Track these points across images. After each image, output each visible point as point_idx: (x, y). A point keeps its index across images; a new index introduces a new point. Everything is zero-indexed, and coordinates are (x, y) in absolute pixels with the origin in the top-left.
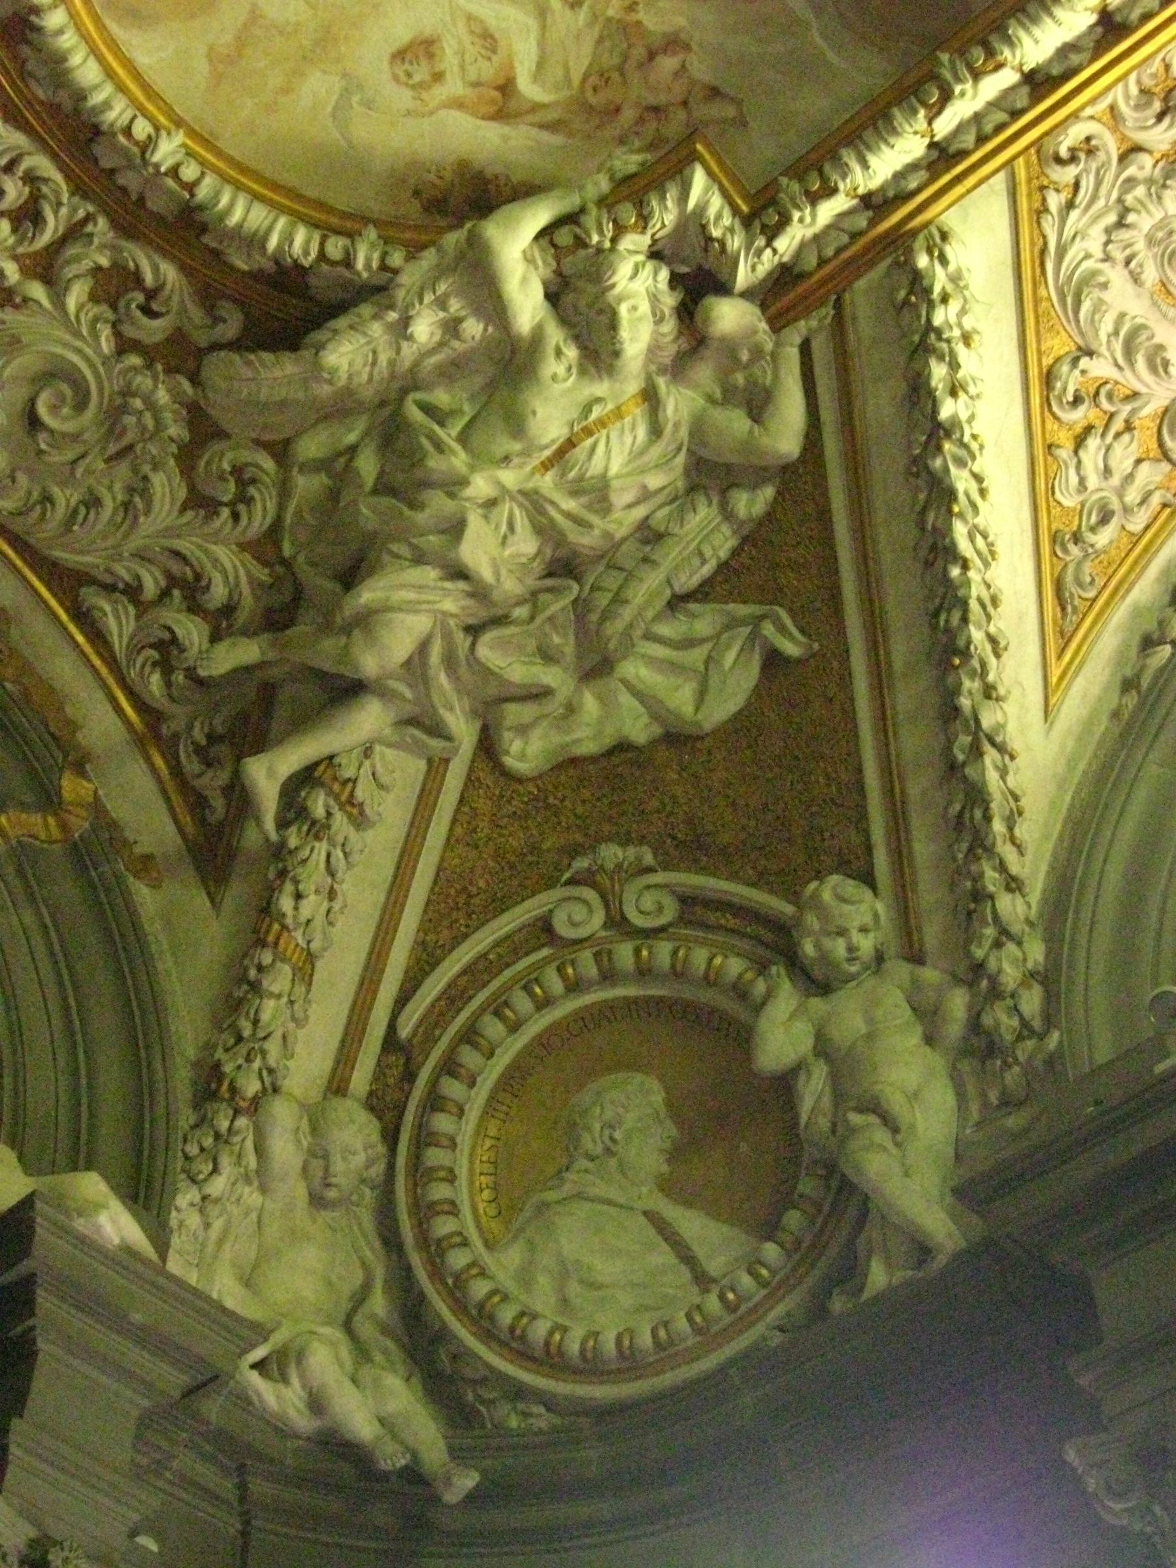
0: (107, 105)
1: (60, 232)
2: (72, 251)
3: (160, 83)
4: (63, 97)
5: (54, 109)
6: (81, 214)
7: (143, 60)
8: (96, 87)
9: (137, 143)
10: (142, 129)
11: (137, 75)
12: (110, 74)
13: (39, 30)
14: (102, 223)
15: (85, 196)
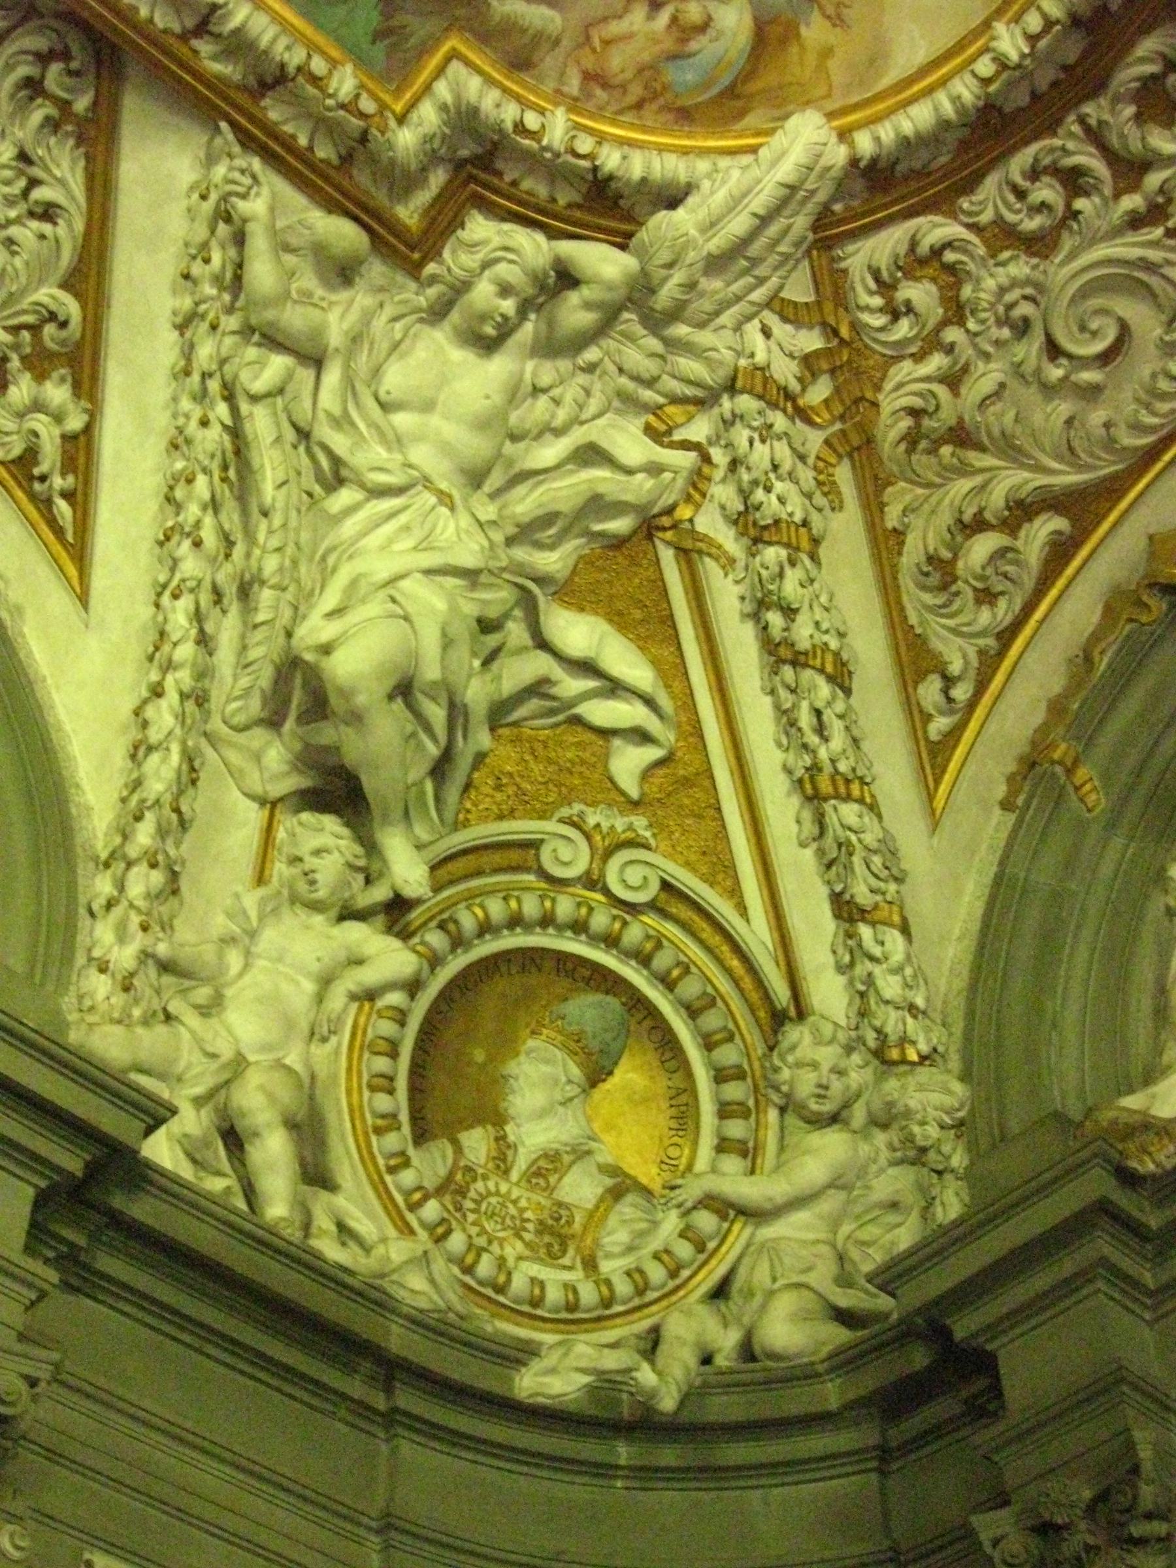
0: (956, 99)
1: (1093, 150)
2: (1114, 141)
3: (946, 42)
4: (951, 138)
5: (964, 145)
6: (1076, 128)
7: (921, 55)
8: (936, 109)
9: (998, 74)
10: (985, 67)
11: (936, 63)
12: (929, 91)
13: (874, 161)
14: (1088, 109)
15: (1059, 122)
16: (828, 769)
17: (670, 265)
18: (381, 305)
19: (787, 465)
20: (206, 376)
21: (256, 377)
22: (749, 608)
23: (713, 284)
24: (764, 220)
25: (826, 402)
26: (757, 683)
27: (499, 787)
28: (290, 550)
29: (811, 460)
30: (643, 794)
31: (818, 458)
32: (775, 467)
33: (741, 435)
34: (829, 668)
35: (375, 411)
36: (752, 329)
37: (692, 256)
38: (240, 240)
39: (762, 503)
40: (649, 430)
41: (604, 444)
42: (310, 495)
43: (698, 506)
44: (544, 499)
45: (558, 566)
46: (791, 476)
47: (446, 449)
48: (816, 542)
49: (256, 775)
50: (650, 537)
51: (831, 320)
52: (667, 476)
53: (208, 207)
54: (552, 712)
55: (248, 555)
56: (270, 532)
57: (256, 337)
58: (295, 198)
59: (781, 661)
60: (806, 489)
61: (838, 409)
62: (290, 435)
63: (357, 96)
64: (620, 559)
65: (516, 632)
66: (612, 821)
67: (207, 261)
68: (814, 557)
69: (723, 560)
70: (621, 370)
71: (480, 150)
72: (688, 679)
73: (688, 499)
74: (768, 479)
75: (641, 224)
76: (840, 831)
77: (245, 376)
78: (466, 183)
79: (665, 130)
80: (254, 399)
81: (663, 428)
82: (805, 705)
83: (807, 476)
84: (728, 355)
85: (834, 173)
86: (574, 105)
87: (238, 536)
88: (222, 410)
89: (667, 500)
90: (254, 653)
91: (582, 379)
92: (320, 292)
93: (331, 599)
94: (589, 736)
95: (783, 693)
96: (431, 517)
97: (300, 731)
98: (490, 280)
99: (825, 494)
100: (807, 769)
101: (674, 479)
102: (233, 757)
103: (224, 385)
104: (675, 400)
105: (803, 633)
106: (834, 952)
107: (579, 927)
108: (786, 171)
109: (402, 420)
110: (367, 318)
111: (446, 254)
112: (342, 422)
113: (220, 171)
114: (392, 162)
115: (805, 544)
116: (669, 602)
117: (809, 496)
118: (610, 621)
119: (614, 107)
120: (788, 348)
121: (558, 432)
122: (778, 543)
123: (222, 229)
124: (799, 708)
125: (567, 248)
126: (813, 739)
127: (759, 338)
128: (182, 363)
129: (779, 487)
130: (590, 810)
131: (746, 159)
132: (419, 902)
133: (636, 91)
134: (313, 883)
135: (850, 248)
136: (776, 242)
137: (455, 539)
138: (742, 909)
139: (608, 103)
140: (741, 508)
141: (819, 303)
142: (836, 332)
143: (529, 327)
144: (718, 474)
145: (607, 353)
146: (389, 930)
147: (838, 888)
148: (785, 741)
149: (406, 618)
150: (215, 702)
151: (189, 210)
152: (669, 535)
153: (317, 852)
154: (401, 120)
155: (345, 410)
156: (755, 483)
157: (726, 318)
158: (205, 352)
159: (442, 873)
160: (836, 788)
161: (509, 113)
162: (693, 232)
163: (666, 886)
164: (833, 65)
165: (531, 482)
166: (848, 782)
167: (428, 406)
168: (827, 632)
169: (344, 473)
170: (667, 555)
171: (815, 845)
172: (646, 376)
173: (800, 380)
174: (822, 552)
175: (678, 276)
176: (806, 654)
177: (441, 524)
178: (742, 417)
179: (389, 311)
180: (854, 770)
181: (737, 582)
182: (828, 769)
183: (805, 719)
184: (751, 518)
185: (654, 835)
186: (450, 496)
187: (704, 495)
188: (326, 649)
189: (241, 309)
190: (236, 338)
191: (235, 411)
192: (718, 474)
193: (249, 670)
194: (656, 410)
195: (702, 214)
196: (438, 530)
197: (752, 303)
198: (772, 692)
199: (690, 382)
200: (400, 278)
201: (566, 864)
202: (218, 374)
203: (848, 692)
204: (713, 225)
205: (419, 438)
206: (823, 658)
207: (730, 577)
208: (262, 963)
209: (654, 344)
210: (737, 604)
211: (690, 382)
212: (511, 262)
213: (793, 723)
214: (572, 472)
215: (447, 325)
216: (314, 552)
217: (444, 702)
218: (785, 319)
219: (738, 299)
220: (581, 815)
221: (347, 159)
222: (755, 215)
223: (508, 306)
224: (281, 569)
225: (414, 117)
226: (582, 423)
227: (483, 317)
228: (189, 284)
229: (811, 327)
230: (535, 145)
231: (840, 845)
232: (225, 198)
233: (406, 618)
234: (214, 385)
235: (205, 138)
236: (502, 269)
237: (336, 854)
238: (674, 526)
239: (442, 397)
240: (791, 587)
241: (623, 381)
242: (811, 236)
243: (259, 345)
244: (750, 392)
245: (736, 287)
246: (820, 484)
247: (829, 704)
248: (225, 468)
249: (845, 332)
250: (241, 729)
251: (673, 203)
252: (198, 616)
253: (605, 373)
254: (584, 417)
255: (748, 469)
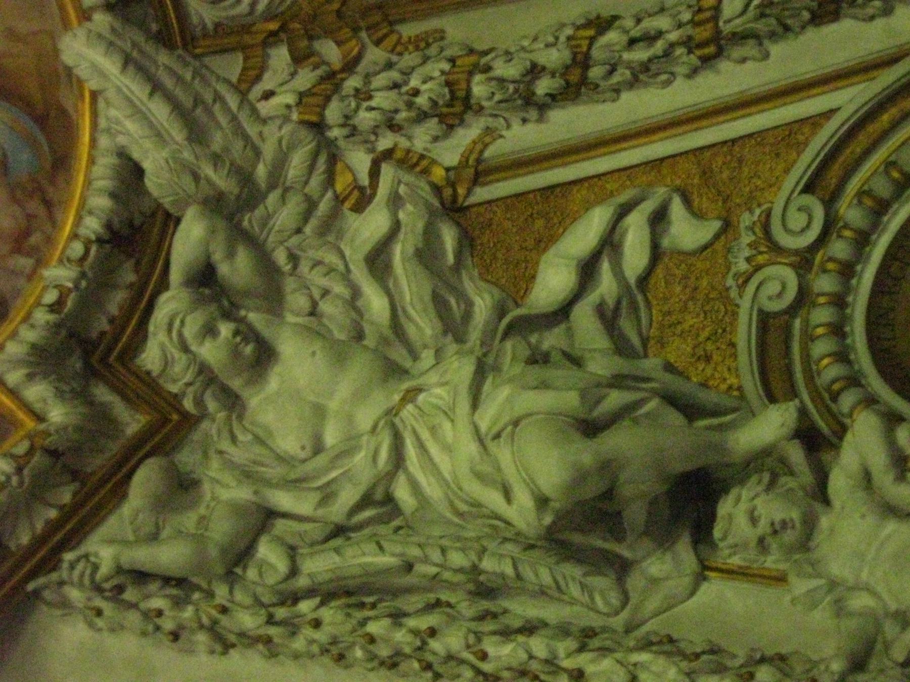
16: (689, 30)
17: (196, 177)
18: (221, 452)
19: (395, 75)
20: (271, 620)
21: (272, 567)
22: (533, 114)
23: (217, 141)
24: (156, 87)
25: (339, 44)
26: (607, 107)
27: (708, 358)
28: (445, 542)
29: (394, 58)
30: (719, 218)
31: (392, 51)
32: (396, 86)
33: (365, 118)
34: (591, 32)
35: (321, 460)
36: (265, 108)
37: (187, 155)
38: (141, 576)
39: (430, 98)
40: (360, 207)
41: (368, 247)
42: (399, 528)
43: (434, 162)
44: (419, 307)
45: (487, 296)
46: (407, 73)
47: (360, 396)
48: (471, 51)
49: (671, 583)
50: (463, 210)
51: (260, 37)
52: (402, 190)
53: (107, 607)
54: (634, 307)
55: (452, 586)
56: (426, 560)
57: (238, 570)
58: (112, 525)
59: (584, 81)
60: (418, 60)
61: (346, 32)
62: (338, 542)
63: (13, 456)
64: (485, 239)
65: (552, 340)
66: (744, 245)
67: (160, 613)
68: (486, 53)
69: (487, 139)
70: (299, 231)
71: (78, 352)
72: (604, 174)
73: (425, 172)
74: (407, 93)
75: (159, 206)
76: (751, 12)
77: (271, 580)
78: (109, 366)
79: (69, 180)
80: (294, 572)
81: (356, 193)
82: (626, 56)
83: (409, 59)
84: (287, 129)
85: (118, 25)
86: (41, 263)
87: (432, 597)
88: (305, 606)
89: (425, 191)
90: (546, 577)
91: (304, 268)
92: (202, 510)
93: (493, 499)
94: (660, 271)
95: (616, 79)
96: (426, 409)
97: (630, 539)
98: (201, 343)
99: (428, 45)
100: (690, 52)
101: (407, 184)
102: (653, 603)
103: (282, 603)
104: (330, 180)
105: (554, 57)
106: (872, 18)
107: (847, 271)
108: (111, 66)
109: (331, 437)
110: (230, 465)
111: (174, 389)
112: (327, 495)
113: (75, 594)
114: (79, 429)
115: (472, 59)
116: (529, 192)
117: (426, 60)
118: (545, 250)
119: (48, 227)
120: (285, 76)
121: (356, 293)
122: (469, 82)
123: (130, 595)
124: (630, 62)
125: (176, 275)
126: (659, 46)
127: (275, 101)
128: (261, 647)
129: (414, 82)
130: (734, 269)
131: (101, 104)
132: (803, 412)
133: (35, 206)
134: (784, 524)
135: (195, 20)
136: (180, 79)
137: (447, 388)
138: (829, 114)
139: (43, 232)
140: (436, 120)
141: (244, 48)
142: (273, 34)
143: (254, 317)
144: (404, 143)
145: (281, 243)
146: (835, 447)
147: (806, 15)
148: (664, 77)
149: (516, 423)
150: (596, 622)
151: (112, 630)
152: (461, 191)
153: (754, 520)
154: (40, 418)
155: (318, 488)
156: (410, 105)
157: (252, 130)
158: (248, 621)
159: (777, 387)
160: (707, 21)
161: (42, 317)
162: (165, 154)
163: (809, 188)
164: (23, 27)
165: (403, 320)
166: (700, 10)
167: (320, 412)
168: (557, 38)
169: (379, 495)
170: (482, 194)
171: (766, 42)
172: (304, 206)
173: (316, 67)
174: (480, 46)
175: (208, 170)
176: (575, 55)
177: (434, 401)
178: (347, 117)
179: (225, 445)
180: (690, 7)
181: (509, 126)
182: (689, 30)
183: (640, 54)
184: (445, 110)
185: (759, 205)
186: (408, 391)
187: (422, 157)
188: (542, 502)
189: (210, 583)
190: (237, 588)
191: (310, 593)
192: (404, 143)
193: (562, 583)
194: (339, 200)
195: (148, 144)
196: (440, 403)
197: (240, 107)
198: (617, 91)
199: (312, 168)
200: (196, 436)
201: (784, 286)
202: (271, 609)
203: (615, 18)
204: (159, 135)
205: (350, 419)
206: (582, 38)
207: (504, 133)
208: (864, 575)
209: (273, 198)
210: (530, 126)
211: (312, 168)
212: (182, 322)
213: (645, 67)
214: (396, 280)
215: (245, 394)
216: (457, 525)
217: (607, 390)
218: (258, 78)
219: (234, 119)
220: (737, 276)
221: (75, 475)
222: (151, 94)
223: (225, 329)
224: (463, 550)
225: (37, 406)
226: (348, 270)
227: (235, 353)
228: (184, 635)
229: (268, 56)
230: (73, 295)
231: (763, 15)
232: (98, 589)
233: (516, 423)
234: (281, 613)
235: (45, 608)
236: (189, 332)
237: (758, 502)
238: (453, 185)
239: (312, 398)
240: (510, 70)
241: (308, 230)
242: (180, 51)
243: (245, 568)
244: (324, 107)
245: (223, 121)
246: (417, 48)
247: (626, 32)
248: (362, 605)
249: (273, 26)
250: (626, 600)
251: (138, 171)
252: (506, 634)
253: (300, 247)
254: (341, 267)
255: (396, 111)
